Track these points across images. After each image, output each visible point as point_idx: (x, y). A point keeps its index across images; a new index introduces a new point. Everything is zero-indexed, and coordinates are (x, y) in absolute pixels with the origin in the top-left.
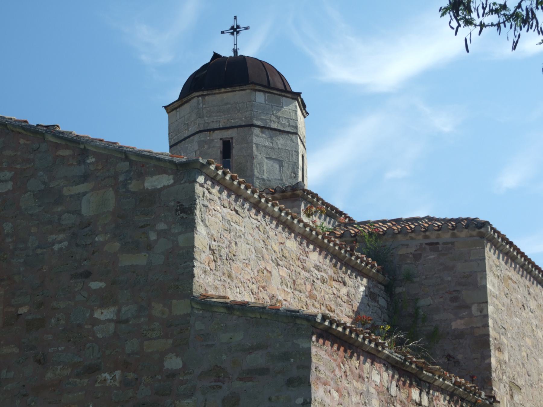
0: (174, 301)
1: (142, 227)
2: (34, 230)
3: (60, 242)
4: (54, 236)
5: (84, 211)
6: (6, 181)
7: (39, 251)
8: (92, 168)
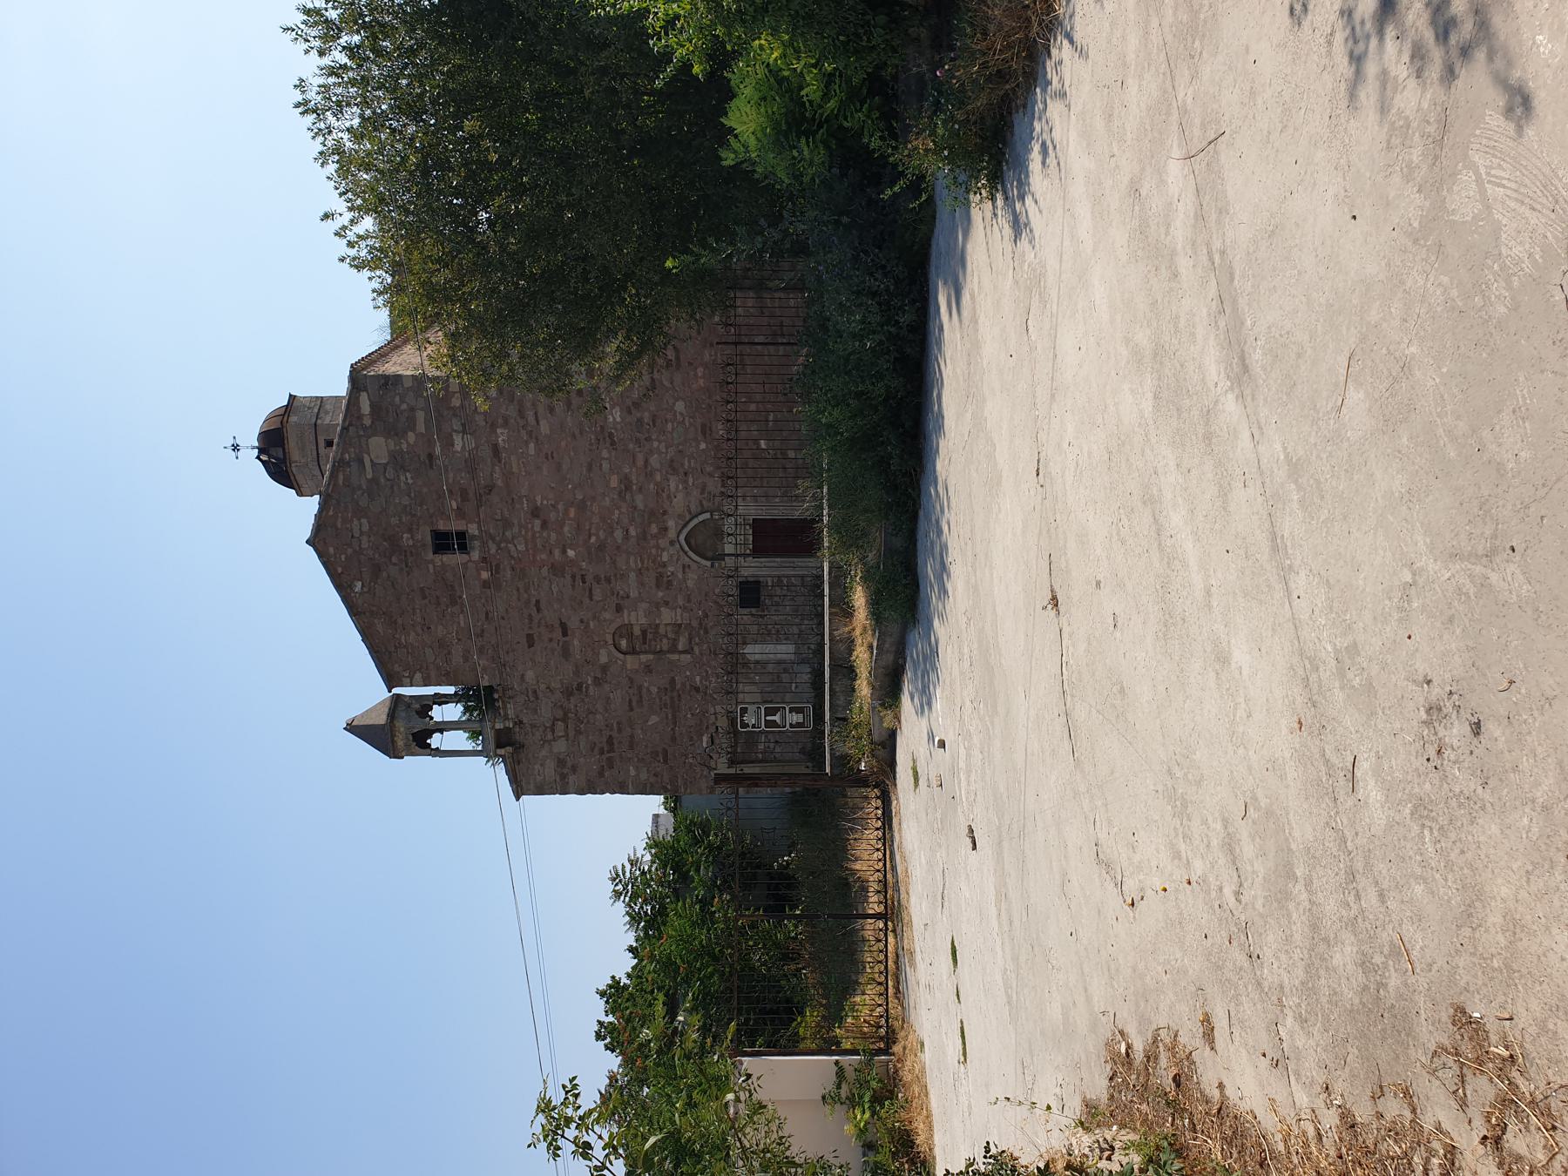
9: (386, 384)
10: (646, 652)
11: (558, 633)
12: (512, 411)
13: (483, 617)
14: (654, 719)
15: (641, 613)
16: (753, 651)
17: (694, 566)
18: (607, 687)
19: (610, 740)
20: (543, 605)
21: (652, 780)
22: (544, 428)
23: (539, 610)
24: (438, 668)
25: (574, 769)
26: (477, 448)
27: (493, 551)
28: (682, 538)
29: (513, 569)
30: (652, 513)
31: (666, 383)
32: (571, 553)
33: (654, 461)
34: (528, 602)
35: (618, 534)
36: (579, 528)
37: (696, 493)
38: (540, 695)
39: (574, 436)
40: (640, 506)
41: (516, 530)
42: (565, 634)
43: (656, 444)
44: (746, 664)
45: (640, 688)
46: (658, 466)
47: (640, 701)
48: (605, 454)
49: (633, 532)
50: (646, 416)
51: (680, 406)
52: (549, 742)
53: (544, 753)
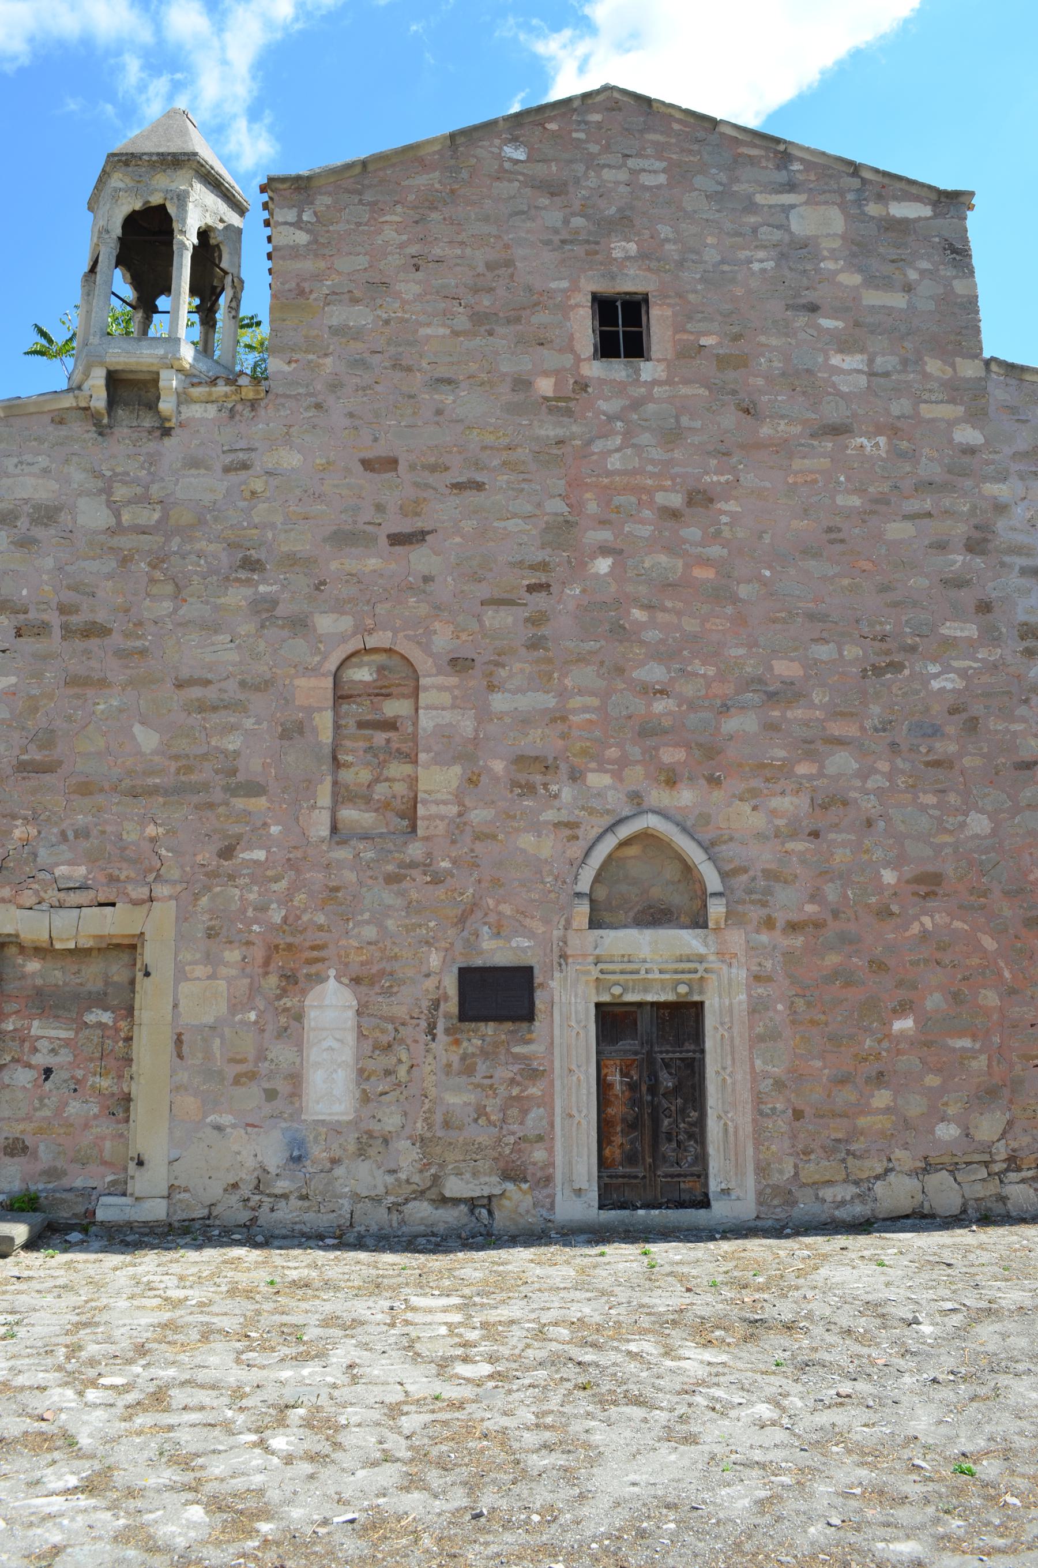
0: (958, 360)
1: (893, 261)
2: (710, 240)
3: (763, 262)
4: (748, 253)
5: (795, 226)
6: (655, 172)
7: (726, 268)
8: (800, 177)
9: (955, 251)
10: (337, 727)
11: (406, 526)
12: (929, 468)
13: (443, 372)
16: (331, 1008)
17: (576, 851)
18: (246, 628)
19: (94, 631)
20: (471, 497)
22: (897, 530)
23: (458, 486)
24: (318, 277)
25: (25, 543)
26: (839, 394)
27: (603, 405)
28: (652, 822)
29: (560, 442)
30: (711, 752)
31: (1028, 793)
32: (603, 565)
33: (842, 762)
35: (655, 673)
36: (669, 586)
37: (764, 856)
38: (234, 478)
39: (884, 589)
40: (732, 724)
41: (657, 453)
42: (397, 540)
43: (884, 766)
44: (290, 979)
45: (237, 706)
46: (831, 769)
47: (202, 707)
48: (851, 652)
49: (660, 706)
51: (979, 824)
52: (108, 491)
53: (78, 477)
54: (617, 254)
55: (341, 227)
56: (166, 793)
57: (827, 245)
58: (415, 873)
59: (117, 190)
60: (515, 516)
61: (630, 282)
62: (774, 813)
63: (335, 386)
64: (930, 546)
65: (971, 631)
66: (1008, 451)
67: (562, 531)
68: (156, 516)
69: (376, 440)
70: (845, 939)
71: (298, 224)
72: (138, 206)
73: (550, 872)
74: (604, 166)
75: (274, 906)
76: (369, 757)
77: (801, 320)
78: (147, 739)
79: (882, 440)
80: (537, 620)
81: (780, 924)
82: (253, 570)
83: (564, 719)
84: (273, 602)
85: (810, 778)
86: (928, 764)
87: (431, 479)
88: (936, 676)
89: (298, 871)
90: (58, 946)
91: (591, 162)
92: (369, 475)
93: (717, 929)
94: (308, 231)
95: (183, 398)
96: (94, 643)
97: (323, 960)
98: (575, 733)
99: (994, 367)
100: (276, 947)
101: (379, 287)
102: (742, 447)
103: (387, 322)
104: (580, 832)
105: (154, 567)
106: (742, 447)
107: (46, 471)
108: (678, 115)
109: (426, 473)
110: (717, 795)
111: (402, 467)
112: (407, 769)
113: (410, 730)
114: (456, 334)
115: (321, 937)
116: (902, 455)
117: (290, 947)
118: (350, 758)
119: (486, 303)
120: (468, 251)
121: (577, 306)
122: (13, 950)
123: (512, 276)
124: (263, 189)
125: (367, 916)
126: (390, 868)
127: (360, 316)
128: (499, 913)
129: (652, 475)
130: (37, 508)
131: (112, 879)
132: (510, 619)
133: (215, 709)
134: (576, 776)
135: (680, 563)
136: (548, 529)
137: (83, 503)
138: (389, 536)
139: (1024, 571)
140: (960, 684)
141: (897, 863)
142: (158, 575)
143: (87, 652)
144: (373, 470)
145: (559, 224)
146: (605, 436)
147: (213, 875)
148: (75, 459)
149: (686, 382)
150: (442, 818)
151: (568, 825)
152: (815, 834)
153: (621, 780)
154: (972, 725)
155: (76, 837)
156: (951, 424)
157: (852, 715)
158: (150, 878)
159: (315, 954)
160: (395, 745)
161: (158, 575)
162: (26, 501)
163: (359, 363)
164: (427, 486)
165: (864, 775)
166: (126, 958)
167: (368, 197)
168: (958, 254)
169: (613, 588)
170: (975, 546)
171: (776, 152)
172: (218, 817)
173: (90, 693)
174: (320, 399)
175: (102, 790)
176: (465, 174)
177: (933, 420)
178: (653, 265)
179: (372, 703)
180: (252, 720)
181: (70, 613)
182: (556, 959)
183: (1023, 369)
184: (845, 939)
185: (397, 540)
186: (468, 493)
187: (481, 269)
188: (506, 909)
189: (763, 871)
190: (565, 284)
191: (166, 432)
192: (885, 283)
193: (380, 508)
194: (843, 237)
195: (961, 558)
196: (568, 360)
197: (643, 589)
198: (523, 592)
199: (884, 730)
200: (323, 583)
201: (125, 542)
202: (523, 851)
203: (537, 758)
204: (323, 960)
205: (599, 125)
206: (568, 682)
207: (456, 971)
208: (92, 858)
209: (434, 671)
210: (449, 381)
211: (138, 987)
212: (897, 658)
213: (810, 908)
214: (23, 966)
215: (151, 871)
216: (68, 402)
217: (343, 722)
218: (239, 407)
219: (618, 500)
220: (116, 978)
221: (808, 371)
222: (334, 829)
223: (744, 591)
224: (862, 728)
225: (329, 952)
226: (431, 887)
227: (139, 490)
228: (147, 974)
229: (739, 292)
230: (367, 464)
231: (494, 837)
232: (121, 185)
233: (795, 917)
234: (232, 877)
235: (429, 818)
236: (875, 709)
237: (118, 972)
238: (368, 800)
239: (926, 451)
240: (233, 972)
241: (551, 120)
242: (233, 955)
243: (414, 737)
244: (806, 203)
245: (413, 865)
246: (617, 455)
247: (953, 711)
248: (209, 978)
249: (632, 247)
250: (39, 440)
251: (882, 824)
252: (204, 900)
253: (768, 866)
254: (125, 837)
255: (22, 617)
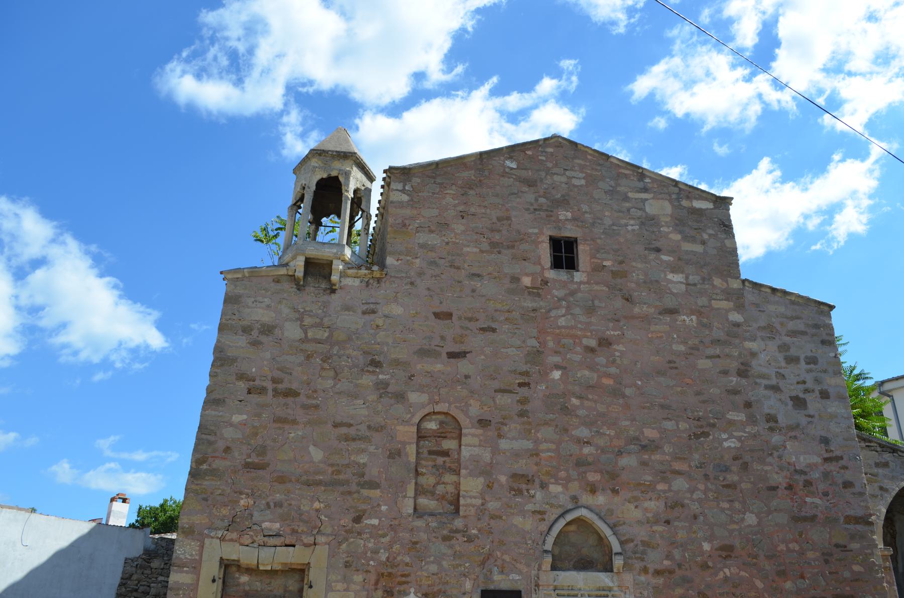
2: (607, 214)
3: (633, 226)
4: (625, 221)
5: (648, 209)
7: (615, 228)
8: (650, 185)
10: (418, 453)
11: (456, 348)
13: (475, 270)
14: (317, 455)
15: (476, 451)
17: (544, 527)
18: (372, 397)
19: (291, 393)
20: (490, 336)
21: (221, 445)
22: (704, 364)
24: (413, 218)
25: (255, 343)
26: (672, 293)
27: (555, 292)
28: (583, 512)
29: (534, 310)
30: (613, 476)
31: (774, 503)
32: (557, 374)
33: (680, 484)
34: (493, 319)
35: (583, 432)
37: (641, 533)
38: (367, 317)
39: (698, 394)
40: (624, 461)
41: (583, 318)
42: (452, 355)
43: (701, 487)
47: (347, 438)
48: (683, 425)
49: (586, 450)
50: (733, 478)
51: (751, 519)
52: (301, 319)
53: (286, 311)
54: (561, 217)
55: (425, 194)
56: (326, 485)
57: (664, 219)
58: (458, 536)
59: (315, 167)
60: (512, 346)
61: (569, 232)
62: (646, 510)
63: (421, 274)
64: (720, 372)
65: (741, 417)
66: (755, 325)
67: (535, 356)
68: (326, 334)
69: (441, 303)
70: (685, 580)
71: (403, 191)
72: (325, 176)
73: (530, 538)
74: (555, 174)
75: (382, 551)
76: (434, 470)
77: (652, 256)
78: (317, 455)
79: (694, 318)
80: (523, 401)
81: (651, 571)
82: (376, 367)
83: (537, 455)
84: (386, 384)
85: (664, 492)
86: (724, 486)
87: (471, 325)
88: (726, 440)
89: (396, 532)
90: (261, 568)
91: (548, 171)
92: (438, 321)
93: (618, 573)
94: (408, 195)
95: (343, 275)
96: (290, 400)
97: (407, 583)
98: (543, 462)
99: (747, 284)
100: (383, 574)
101: (444, 226)
102: (625, 317)
103: (447, 243)
104: (546, 517)
105: (324, 362)
106: (625, 317)
107: (268, 306)
108: (590, 152)
109: (467, 322)
110: (617, 499)
111: (454, 318)
112: (454, 478)
113: (456, 457)
114: (482, 252)
115: (408, 570)
116: (705, 326)
117: (390, 575)
118: (424, 471)
119: (497, 237)
120: (488, 211)
121: (543, 242)
122: (234, 569)
123: (510, 225)
124: (385, 171)
125: (432, 559)
126: (445, 532)
127: (434, 240)
128: (503, 560)
129: (581, 330)
130: (263, 325)
131: (294, 532)
132: (509, 400)
133: (354, 440)
134: (543, 486)
135: (595, 375)
136: (528, 354)
137: (287, 325)
138: (447, 353)
139: (767, 387)
140: (738, 445)
141: (710, 539)
142: (326, 366)
143: (286, 405)
144: (440, 318)
145: (533, 201)
146: (557, 308)
147: (349, 532)
148: (284, 301)
149: (597, 283)
150: (473, 506)
151: (540, 513)
152: (668, 522)
153: (567, 489)
154: (745, 466)
155: (275, 506)
156: (728, 311)
157: (684, 459)
158: (315, 532)
159: (404, 579)
160: (448, 465)
161: (326, 366)
162: (257, 321)
163: (433, 263)
164: (467, 328)
165: (692, 491)
166: (297, 577)
167: (438, 180)
168: (727, 227)
169: (562, 386)
170: (743, 373)
171: (638, 173)
172: (353, 499)
173: (287, 427)
174: (413, 279)
175: (291, 481)
176: (486, 173)
177: (718, 309)
178: (580, 224)
179: (438, 442)
180: (374, 447)
181: (278, 383)
182: (533, 587)
183: (761, 285)
184: (685, 580)
185: (452, 355)
186: (488, 333)
187: (495, 220)
188: (507, 558)
189: (641, 541)
190: (536, 231)
191: (333, 291)
192: (693, 240)
193: (443, 338)
194: (671, 216)
195: (735, 379)
196: (538, 269)
197: (577, 388)
198: (516, 386)
199: (701, 467)
200: (413, 376)
201: (310, 347)
202: (516, 526)
203: (523, 475)
204: (407, 583)
205: (552, 154)
206: (539, 435)
207: (479, 591)
208: (283, 518)
209: (470, 426)
210: (479, 275)
211: (304, 594)
212: (706, 430)
213: (666, 563)
214: (239, 578)
215: (315, 528)
216: (283, 271)
217: (421, 451)
218: (371, 281)
219: (564, 341)
220: (290, 588)
221: (657, 281)
222: (415, 509)
223: (628, 392)
224: (690, 466)
225: (411, 578)
226: (467, 544)
227: (318, 320)
228: (311, 587)
229: (622, 240)
230: (437, 315)
231: (501, 517)
232: (317, 165)
233: (659, 567)
234: (359, 534)
235: (466, 505)
236: (696, 456)
237: (292, 584)
238: (433, 493)
239: (716, 324)
240: (358, 588)
241: (529, 149)
242: (358, 578)
243: (458, 461)
244: (653, 198)
245: (457, 531)
246: (563, 318)
247: (735, 458)
248: (344, 590)
249: (569, 215)
250: (266, 290)
251: (702, 518)
252: (344, 546)
253: (643, 539)
254: (302, 508)
255: (252, 383)
